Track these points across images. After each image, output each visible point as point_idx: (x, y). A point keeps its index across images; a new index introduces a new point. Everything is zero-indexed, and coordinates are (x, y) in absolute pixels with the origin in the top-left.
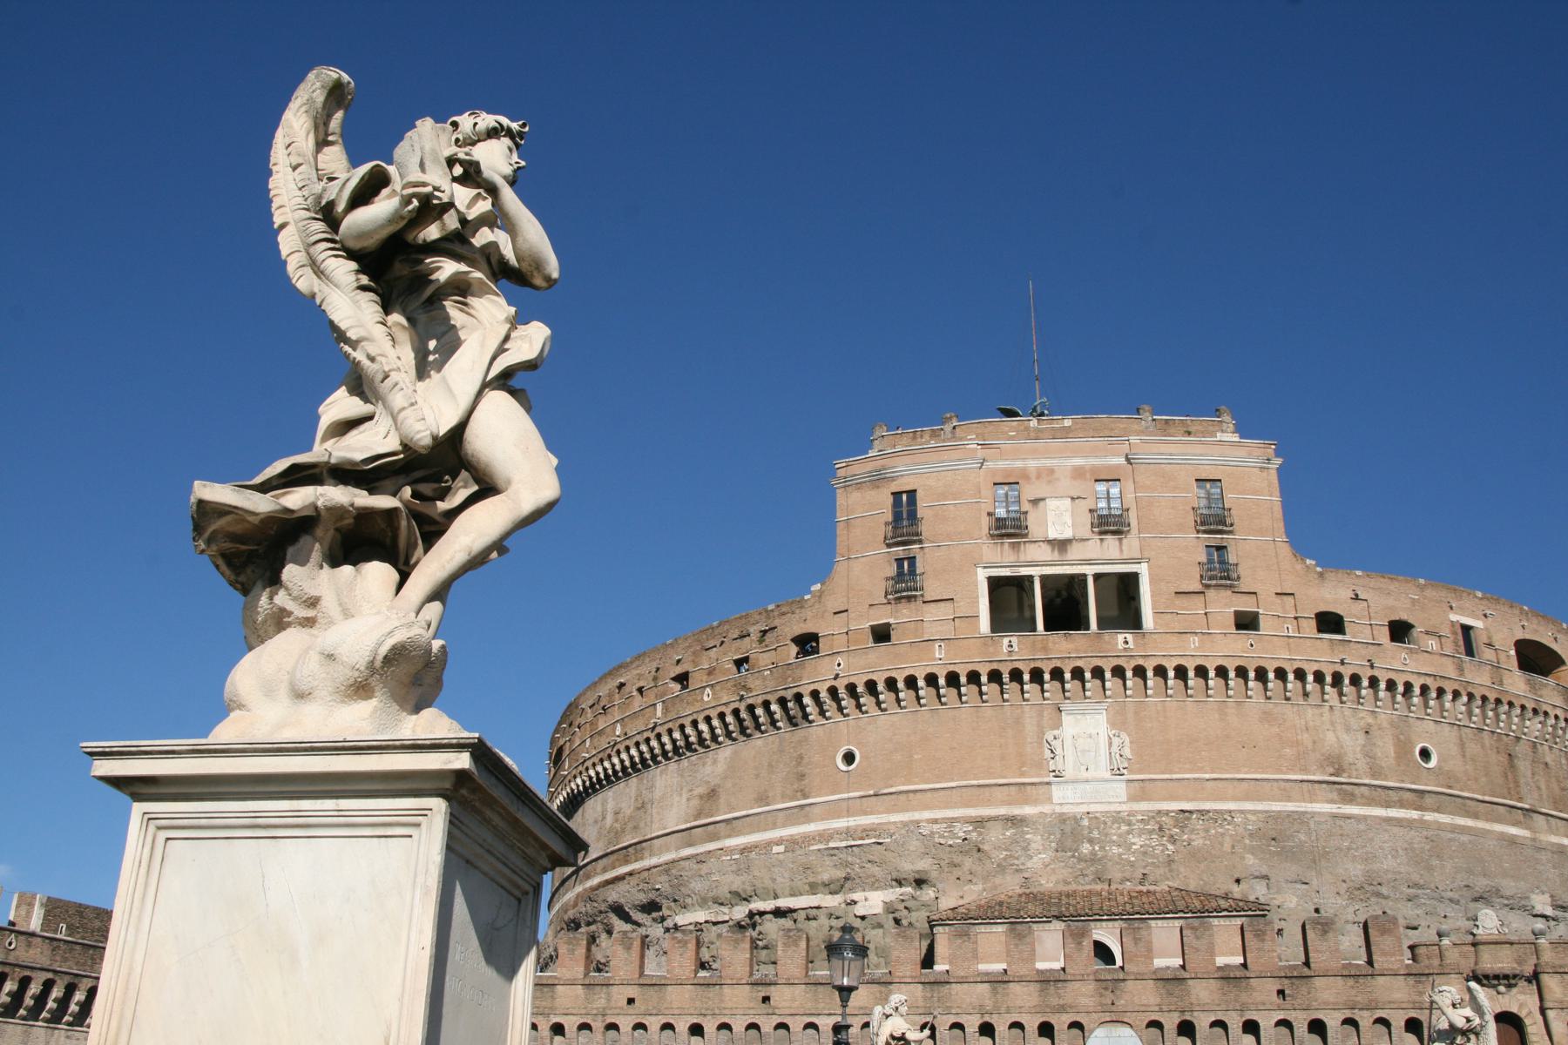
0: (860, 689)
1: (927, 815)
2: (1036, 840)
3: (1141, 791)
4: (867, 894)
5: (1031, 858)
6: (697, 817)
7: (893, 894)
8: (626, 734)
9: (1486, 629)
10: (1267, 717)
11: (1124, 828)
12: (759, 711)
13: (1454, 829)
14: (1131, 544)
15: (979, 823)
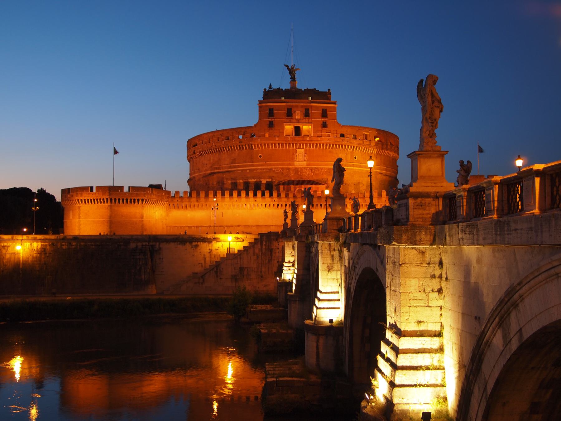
0: (263, 145)
1: (274, 167)
2: (291, 172)
3: (308, 165)
4: (264, 180)
5: (290, 174)
6: (232, 164)
7: (268, 180)
8: (215, 146)
9: (369, 134)
10: (330, 152)
11: (306, 170)
12: (244, 146)
13: (358, 170)
14: (310, 121)
15: (283, 169)
